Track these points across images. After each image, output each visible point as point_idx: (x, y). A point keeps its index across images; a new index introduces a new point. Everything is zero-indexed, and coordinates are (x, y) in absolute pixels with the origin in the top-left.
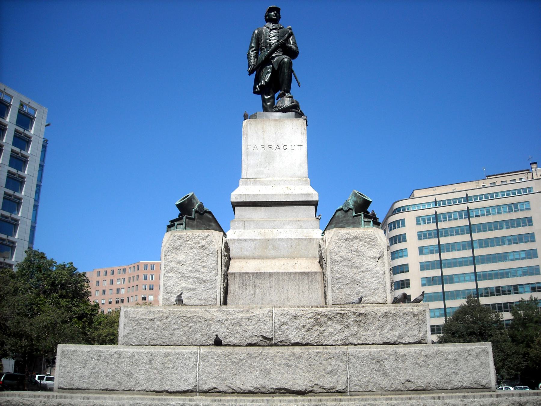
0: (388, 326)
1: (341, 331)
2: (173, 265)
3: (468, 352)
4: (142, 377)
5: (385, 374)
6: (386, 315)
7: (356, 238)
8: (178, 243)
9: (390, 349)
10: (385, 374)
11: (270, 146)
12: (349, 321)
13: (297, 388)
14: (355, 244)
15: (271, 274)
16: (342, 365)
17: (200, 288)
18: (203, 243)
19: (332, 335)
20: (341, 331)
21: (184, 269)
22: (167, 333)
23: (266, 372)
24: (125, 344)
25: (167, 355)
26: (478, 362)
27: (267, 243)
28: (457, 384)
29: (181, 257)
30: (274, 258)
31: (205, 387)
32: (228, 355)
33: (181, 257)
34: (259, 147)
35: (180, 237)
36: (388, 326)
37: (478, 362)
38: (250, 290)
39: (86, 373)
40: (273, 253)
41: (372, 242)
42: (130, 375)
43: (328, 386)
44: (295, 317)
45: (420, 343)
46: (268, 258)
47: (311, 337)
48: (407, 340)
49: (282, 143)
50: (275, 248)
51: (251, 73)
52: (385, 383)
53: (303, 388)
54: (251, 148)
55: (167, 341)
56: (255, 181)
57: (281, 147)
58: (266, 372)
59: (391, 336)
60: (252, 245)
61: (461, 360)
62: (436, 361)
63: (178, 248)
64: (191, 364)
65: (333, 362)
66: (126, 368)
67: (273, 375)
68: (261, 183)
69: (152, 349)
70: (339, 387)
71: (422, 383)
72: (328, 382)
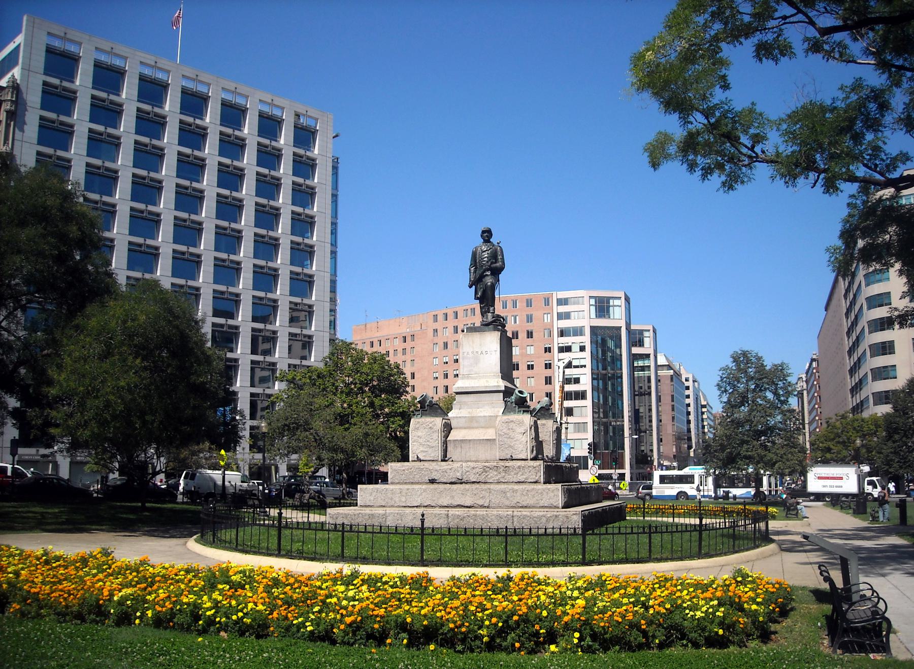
0: (521, 473)
1: (496, 475)
2: (415, 438)
3: (549, 489)
4: (397, 500)
5: (508, 499)
6: (519, 467)
7: (512, 421)
8: (417, 426)
9: (511, 486)
10: (508, 499)
11: (477, 352)
12: (501, 470)
13: (466, 505)
14: (511, 425)
15: (470, 440)
16: (488, 494)
17: (430, 451)
18: (431, 425)
19: (492, 477)
20: (496, 475)
21: (421, 441)
22: (411, 477)
23: (453, 497)
24: (392, 483)
25: (408, 489)
26: (553, 494)
27: (472, 419)
28: (541, 505)
29: (420, 434)
30: (477, 428)
31: (426, 504)
32: (435, 489)
33: (420, 434)
34: (470, 353)
35: (419, 422)
36: (521, 473)
37: (553, 494)
38: (459, 450)
39: (372, 499)
40: (475, 425)
41: (521, 423)
42: (392, 499)
43: (481, 504)
44: (473, 468)
45: (536, 482)
46: (473, 428)
47: (482, 479)
48: (530, 481)
49: (484, 349)
50: (477, 422)
51: (470, 287)
52: (507, 503)
53: (469, 505)
54: (465, 354)
55: (412, 481)
56: (468, 377)
57: (484, 352)
58: (453, 497)
59: (522, 478)
60: (464, 420)
61: (544, 493)
62: (533, 493)
63: (418, 429)
64: (419, 493)
65: (483, 492)
66: (390, 495)
67: (456, 498)
68: (472, 378)
69: (401, 486)
70: (485, 505)
71: (525, 504)
72: (481, 502)
